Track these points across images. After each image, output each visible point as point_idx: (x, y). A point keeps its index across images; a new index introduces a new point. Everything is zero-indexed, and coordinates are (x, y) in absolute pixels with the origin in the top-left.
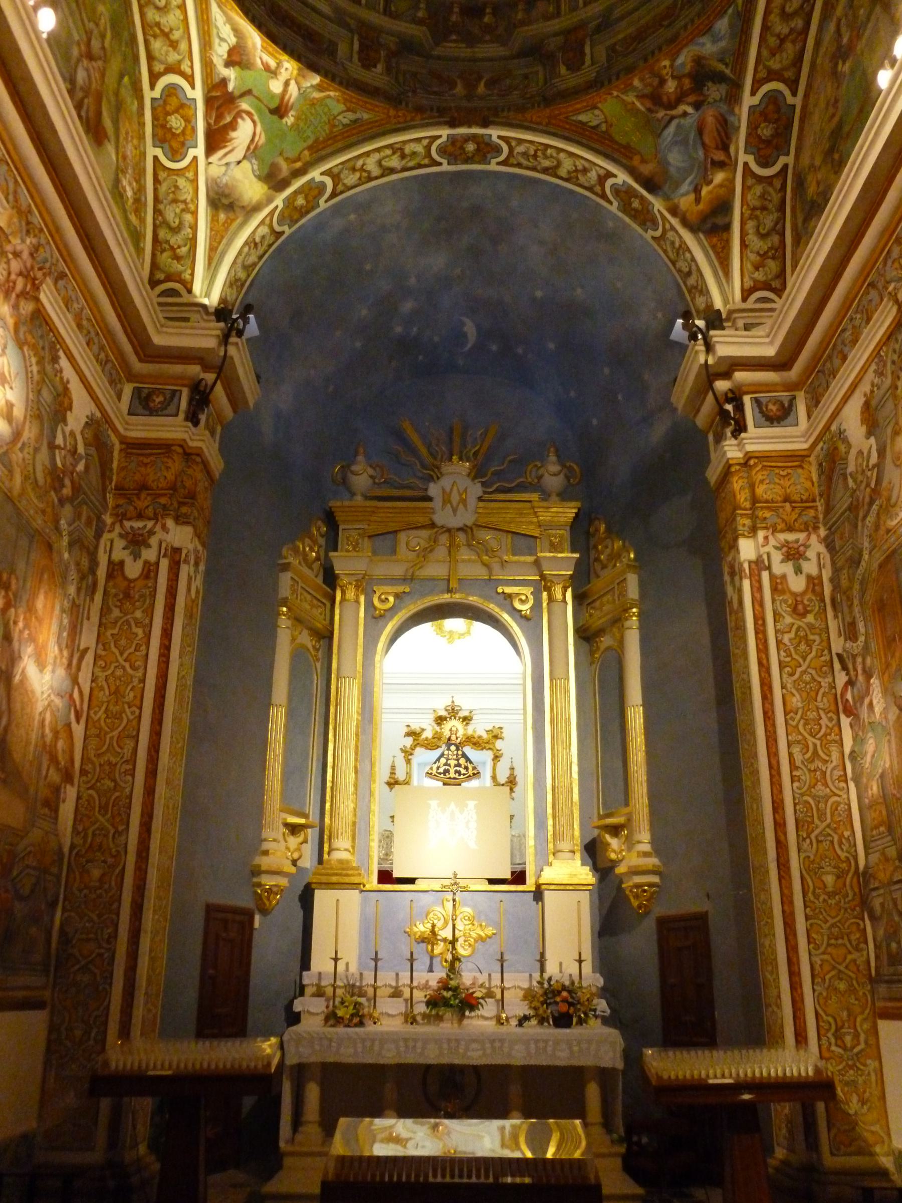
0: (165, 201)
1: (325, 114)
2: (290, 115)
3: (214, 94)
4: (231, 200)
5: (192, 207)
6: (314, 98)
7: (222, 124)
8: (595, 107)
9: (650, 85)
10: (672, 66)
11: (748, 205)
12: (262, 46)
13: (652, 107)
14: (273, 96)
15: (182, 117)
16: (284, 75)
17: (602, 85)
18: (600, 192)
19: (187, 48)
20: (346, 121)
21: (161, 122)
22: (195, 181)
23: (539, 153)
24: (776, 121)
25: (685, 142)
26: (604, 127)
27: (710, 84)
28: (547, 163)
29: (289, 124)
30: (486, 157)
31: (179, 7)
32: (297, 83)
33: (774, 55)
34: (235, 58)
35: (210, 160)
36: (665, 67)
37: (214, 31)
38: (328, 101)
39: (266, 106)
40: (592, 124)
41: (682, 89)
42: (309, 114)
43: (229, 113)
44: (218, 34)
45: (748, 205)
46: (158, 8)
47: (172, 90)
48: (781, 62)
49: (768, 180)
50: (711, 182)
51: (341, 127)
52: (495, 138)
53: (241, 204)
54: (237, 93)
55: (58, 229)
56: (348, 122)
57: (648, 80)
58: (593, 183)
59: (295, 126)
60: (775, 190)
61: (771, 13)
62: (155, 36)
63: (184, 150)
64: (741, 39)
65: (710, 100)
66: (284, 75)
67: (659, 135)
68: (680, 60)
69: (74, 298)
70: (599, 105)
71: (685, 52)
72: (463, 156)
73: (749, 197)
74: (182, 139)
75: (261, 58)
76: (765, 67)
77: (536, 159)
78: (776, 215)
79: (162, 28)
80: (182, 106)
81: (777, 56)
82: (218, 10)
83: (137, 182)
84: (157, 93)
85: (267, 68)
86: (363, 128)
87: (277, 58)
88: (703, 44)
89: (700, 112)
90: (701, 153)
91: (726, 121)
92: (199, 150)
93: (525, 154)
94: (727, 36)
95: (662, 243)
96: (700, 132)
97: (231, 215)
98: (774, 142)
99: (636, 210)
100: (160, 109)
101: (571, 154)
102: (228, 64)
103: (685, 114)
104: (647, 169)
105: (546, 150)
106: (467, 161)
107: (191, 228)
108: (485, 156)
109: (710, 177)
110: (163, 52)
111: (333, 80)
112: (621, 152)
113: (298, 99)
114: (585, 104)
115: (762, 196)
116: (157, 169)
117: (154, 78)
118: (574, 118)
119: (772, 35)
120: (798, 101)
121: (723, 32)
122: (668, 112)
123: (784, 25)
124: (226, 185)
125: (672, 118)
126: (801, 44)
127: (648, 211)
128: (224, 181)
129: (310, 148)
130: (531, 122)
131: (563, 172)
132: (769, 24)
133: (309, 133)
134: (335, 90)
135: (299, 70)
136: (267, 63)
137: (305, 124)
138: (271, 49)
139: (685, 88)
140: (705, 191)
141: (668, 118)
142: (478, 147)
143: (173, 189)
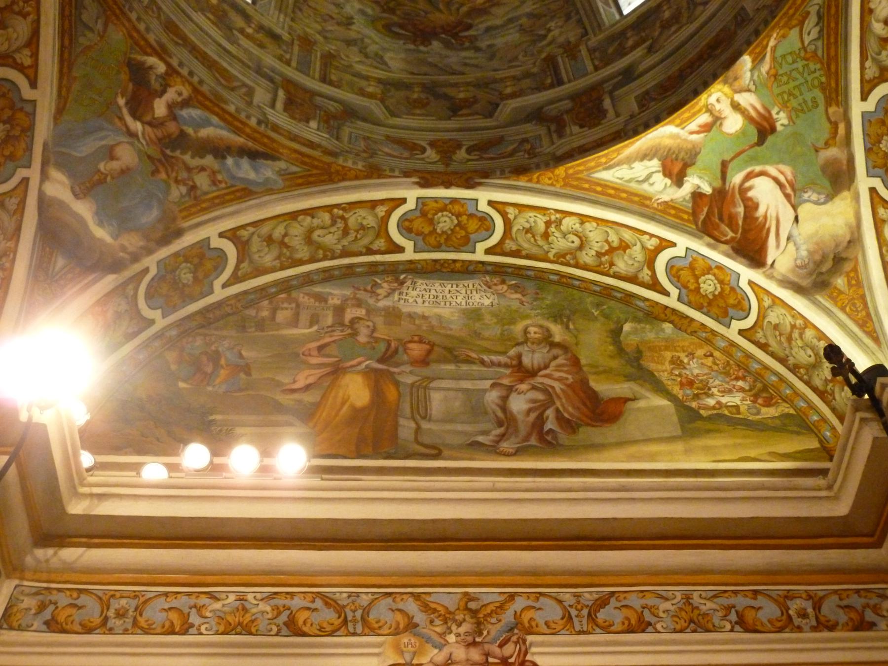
0: (787, 352)
1: (794, 62)
2: (775, 116)
3: (702, 217)
4: (832, 256)
5: (799, 322)
6: (768, 73)
7: (740, 223)
12: (677, 126)
14: (743, 132)
15: (704, 275)
16: (724, 108)
19: (630, 232)
20: (814, 34)
21: (705, 304)
22: (777, 301)
29: (785, 122)
31: (582, 223)
32: (740, 91)
34: (676, 169)
35: (769, 261)
37: (634, 186)
38: (779, 53)
39: (752, 147)
42: (785, 88)
43: (734, 205)
44: (638, 181)
46: (581, 248)
47: (674, 271)
51: (819, 43)
53: (845, 244)
54: (718, 184)
55: (534, 572)
56: (817, 29)
59: (794, 114)
62: (612, 264)
63: (738, 290)
66: (724, 108)
69: (651, 601)
74: (727, 288)
75: (692, 133)
79: (603, 251)
80: (692, 268)
82: (612, 171)
83: (743, 378)
84: (674, 292)
85: (707, 128)
86: (833, 11)
87: (700, 111)
92: (746, 274)
97: (848, 266)
100: (692, 298)
102: (679, 181)
107: (819, 340)
110: (630, 262)
111: (757, 33)
113: (760, 97)
116: (753, 338)
117: (655, 285)
124: (811, 253)
128: (804, 253)
129: (828, 104)
133: (808, 96)
134: (769, 36)
135: (725, 82)
136: (700, 126)
137: (795, 97)
138: (687, 115)
143: (777, 333)
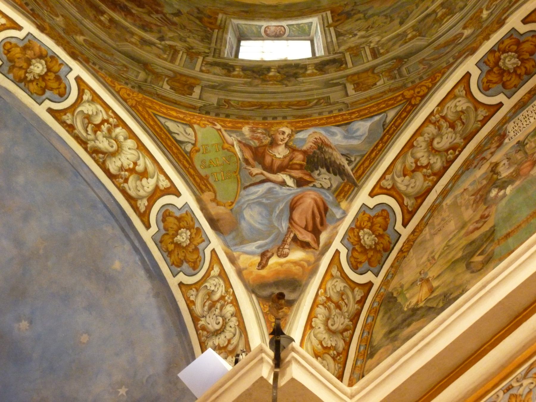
8: (191, 126)
9: (259, 139)
10: (290, 136)
11: (325, 291)
13: (251, 160)
17: (208, 113)
18: (142, 209)
23: (105, 127)
24: (379, 236)
25: (270, 209)
26: (189, 148)
27: (324, 170)
28: (103, 144)
30: (44, 92)
33: (405, 175)
36: (283, 133)
40: (180, 138)
41: (291, 159)
45: (325, 291)
48: (407, 186)
49: (353, 285)
50: (286, 255)
52: (71, 77)
57: (259, 135)
58: (142, 193)
60: (354, 298)
61: (422, 135)
64: (377, 146)
65: (317, 184)
67: (246, 188)
68: (301, 135)
70: (196, 126)
71: (311, 130)
72: (21, 73)
73: (329, 285)
76: (393, 178)
77: (95, 132)
78: (347, 321)
81: (407, 178)
88: (333, 134)
89: (299, 190)
90: (285, 225)
91: (326, 209)
93: (88, 118)
94: (363, 138)
95: (193, 292)
96: (292, 207)
98: (371, 253)
99: (178, 245)
101: (141, 146)
103: (283, 183)
104: (215, 210)
105: (116, 126)
106: (21, 81)
108: (43, 90)
109: (286, 251)
112: (194, 179)
114: (181, 116)
115: (342, 294)
118: (163, 120)
119: (412, 155)
120: (405, 233)
121: (358, 133)
122: (265, 173)
123: (426, 155)
125: (267, 180)
126: (430, 184)
127: (196, 249)
130: (118, 92)
131: (113, 166)
132: (415, 143)
139: (295, 161)
140: (274, 260)
141: (263, 178)
142: (46, 74)
